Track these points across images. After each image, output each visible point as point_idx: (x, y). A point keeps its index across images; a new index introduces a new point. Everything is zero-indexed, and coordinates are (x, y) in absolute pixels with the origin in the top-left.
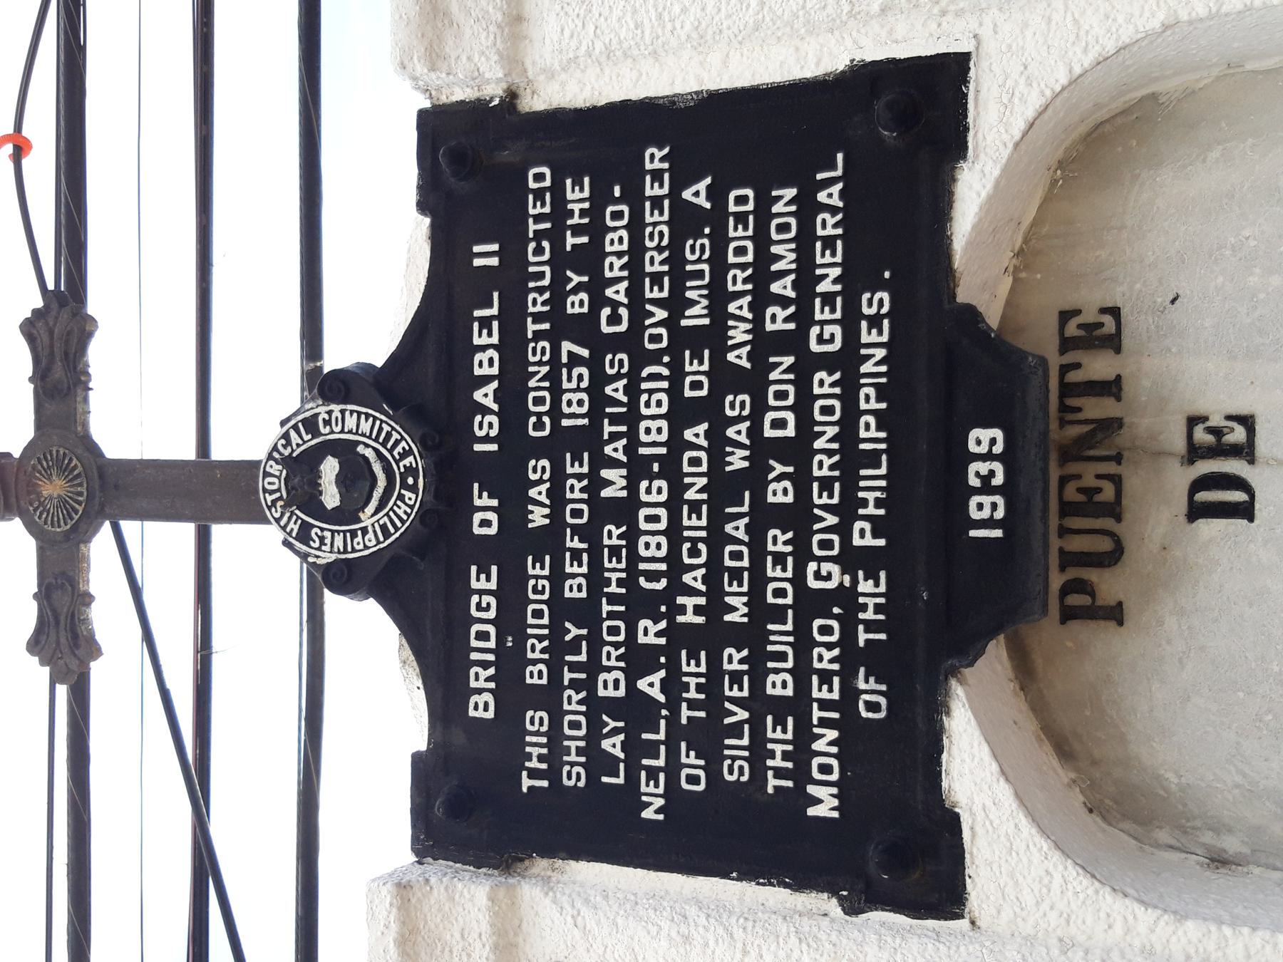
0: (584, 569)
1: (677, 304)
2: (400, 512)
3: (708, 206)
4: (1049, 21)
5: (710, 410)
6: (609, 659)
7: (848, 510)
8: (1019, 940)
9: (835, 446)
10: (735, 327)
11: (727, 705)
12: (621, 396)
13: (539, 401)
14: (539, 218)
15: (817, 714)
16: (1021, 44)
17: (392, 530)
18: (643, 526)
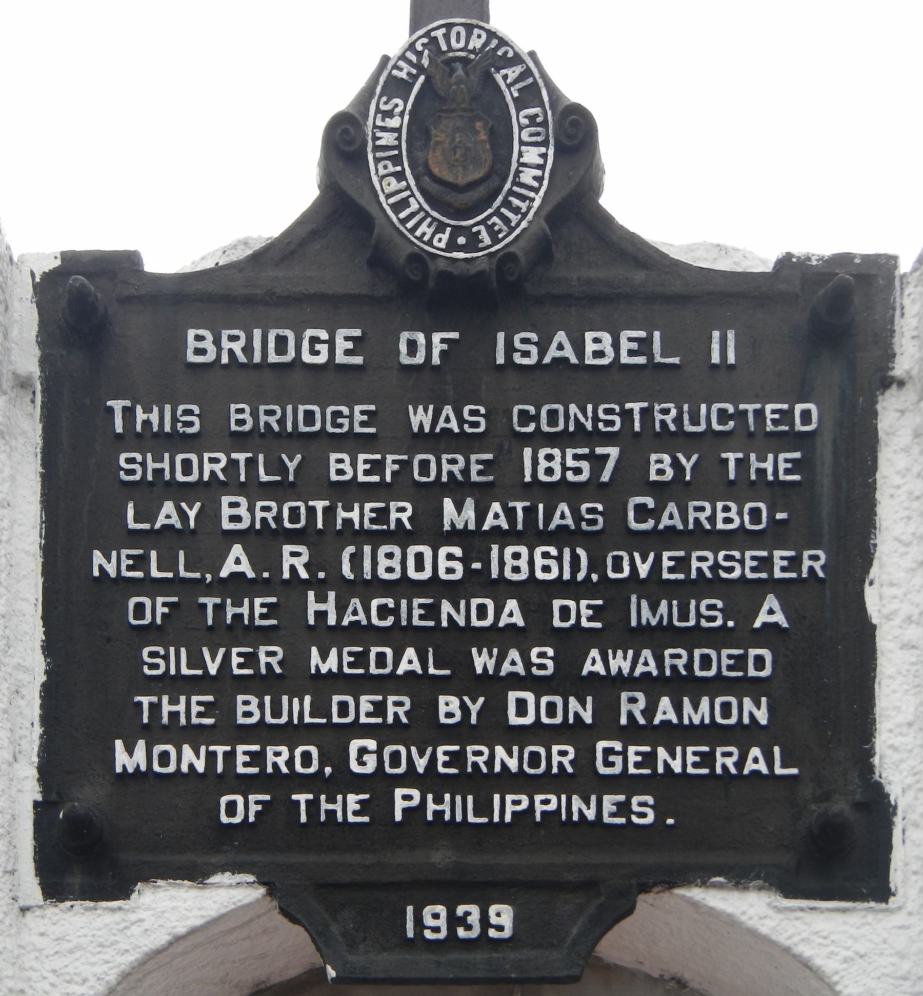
0: (361, 478)
1: (654, 589)
2: (423, 228)
3: (757, 624)
4: (905, 978)
5: (537, 628)
6: (264, 509)
7: (430, 782)
8: (16, 952)
9: (497, 768)
10: (625, 658)
11: (222, 651)
12: (556, 521)
14: (760, 414)
15: (220, 750)
16: (886, 952)
17: (402, 215)
18: (412, 550)
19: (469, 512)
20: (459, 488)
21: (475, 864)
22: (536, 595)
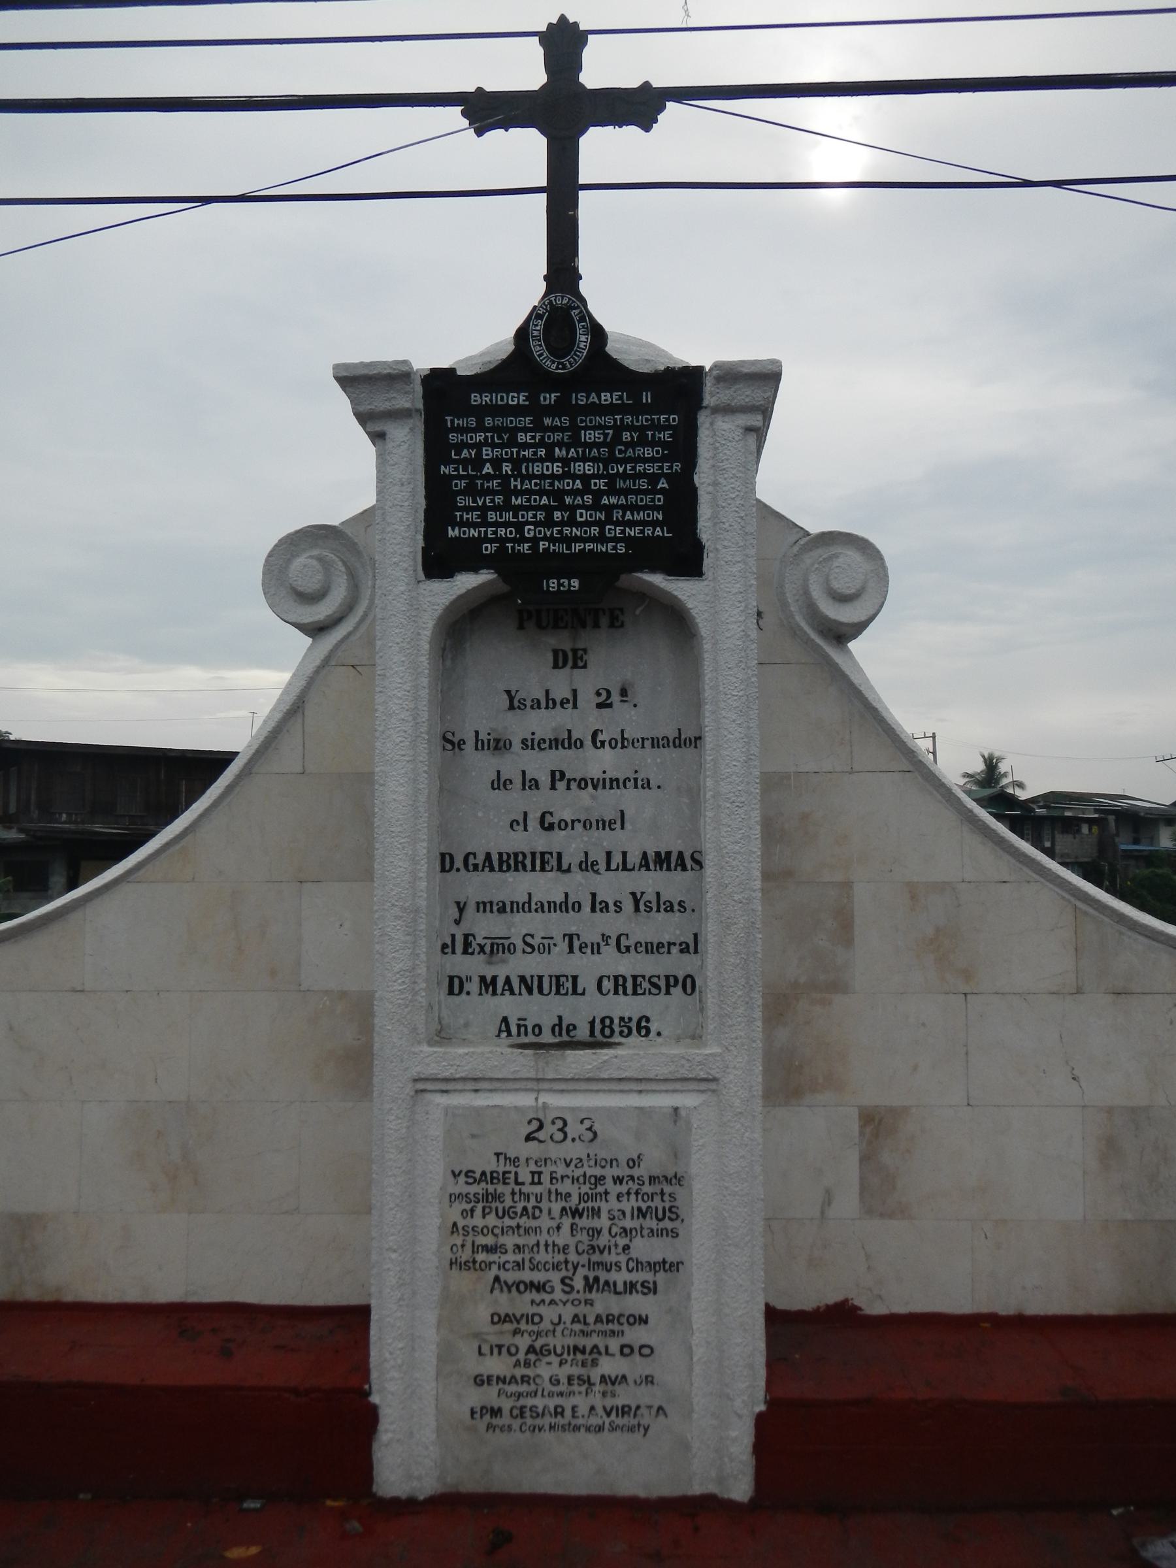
7: (552, 540)
13: (591, 421)
14: (659, 419)
15: (483, 529)
19: (564, 452)
20: (560, 444)
22: (585, 479)
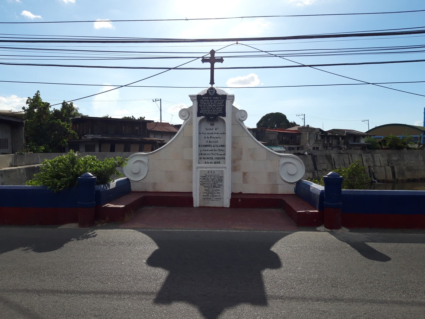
21: (212, 116)
